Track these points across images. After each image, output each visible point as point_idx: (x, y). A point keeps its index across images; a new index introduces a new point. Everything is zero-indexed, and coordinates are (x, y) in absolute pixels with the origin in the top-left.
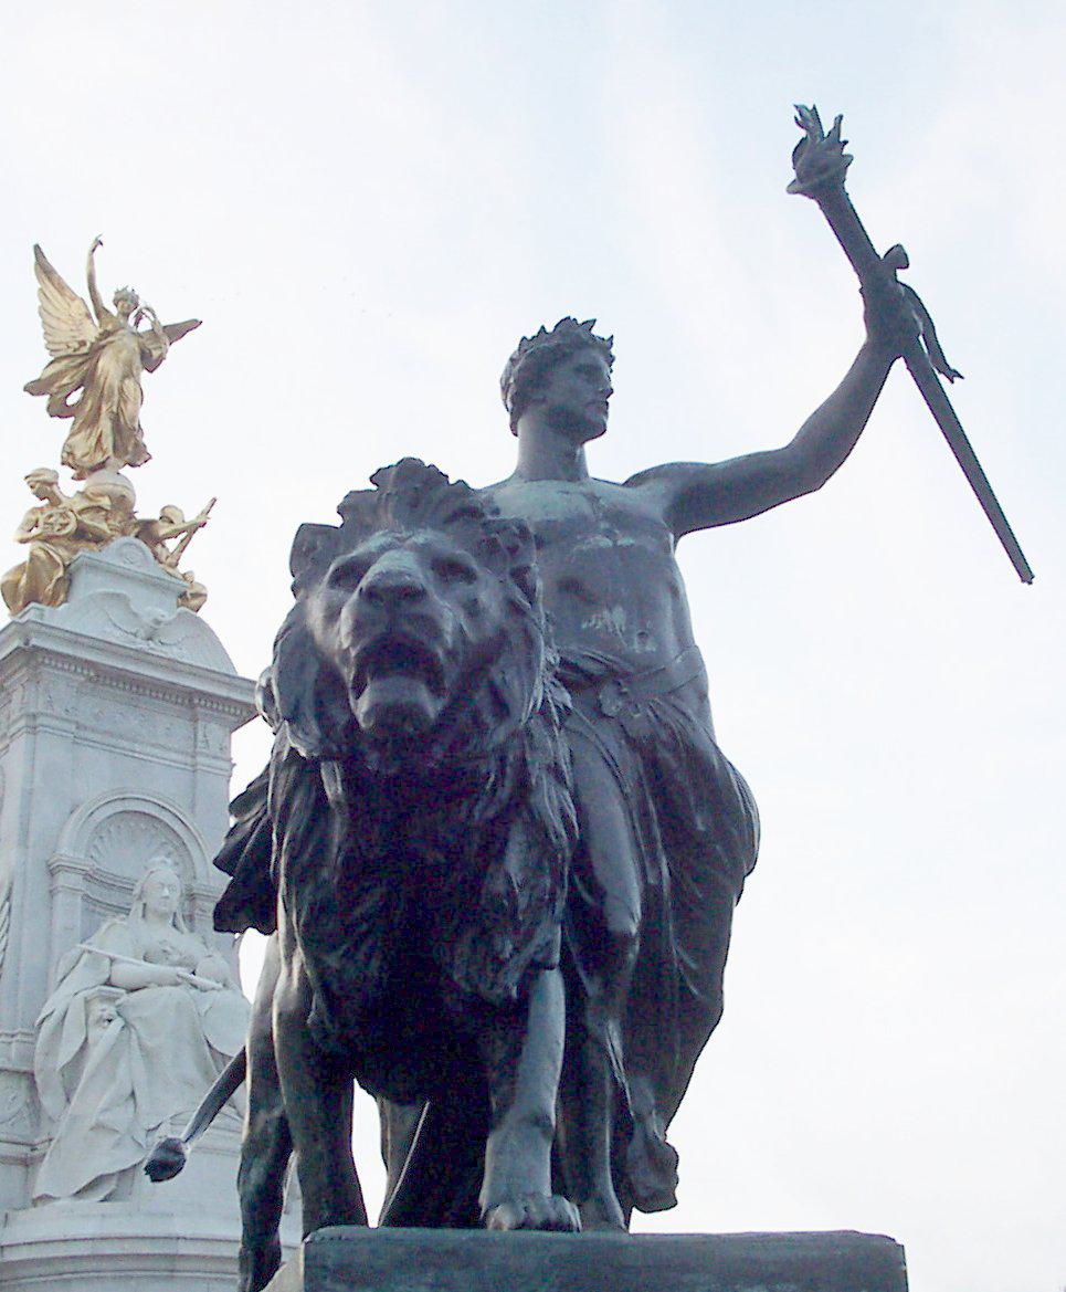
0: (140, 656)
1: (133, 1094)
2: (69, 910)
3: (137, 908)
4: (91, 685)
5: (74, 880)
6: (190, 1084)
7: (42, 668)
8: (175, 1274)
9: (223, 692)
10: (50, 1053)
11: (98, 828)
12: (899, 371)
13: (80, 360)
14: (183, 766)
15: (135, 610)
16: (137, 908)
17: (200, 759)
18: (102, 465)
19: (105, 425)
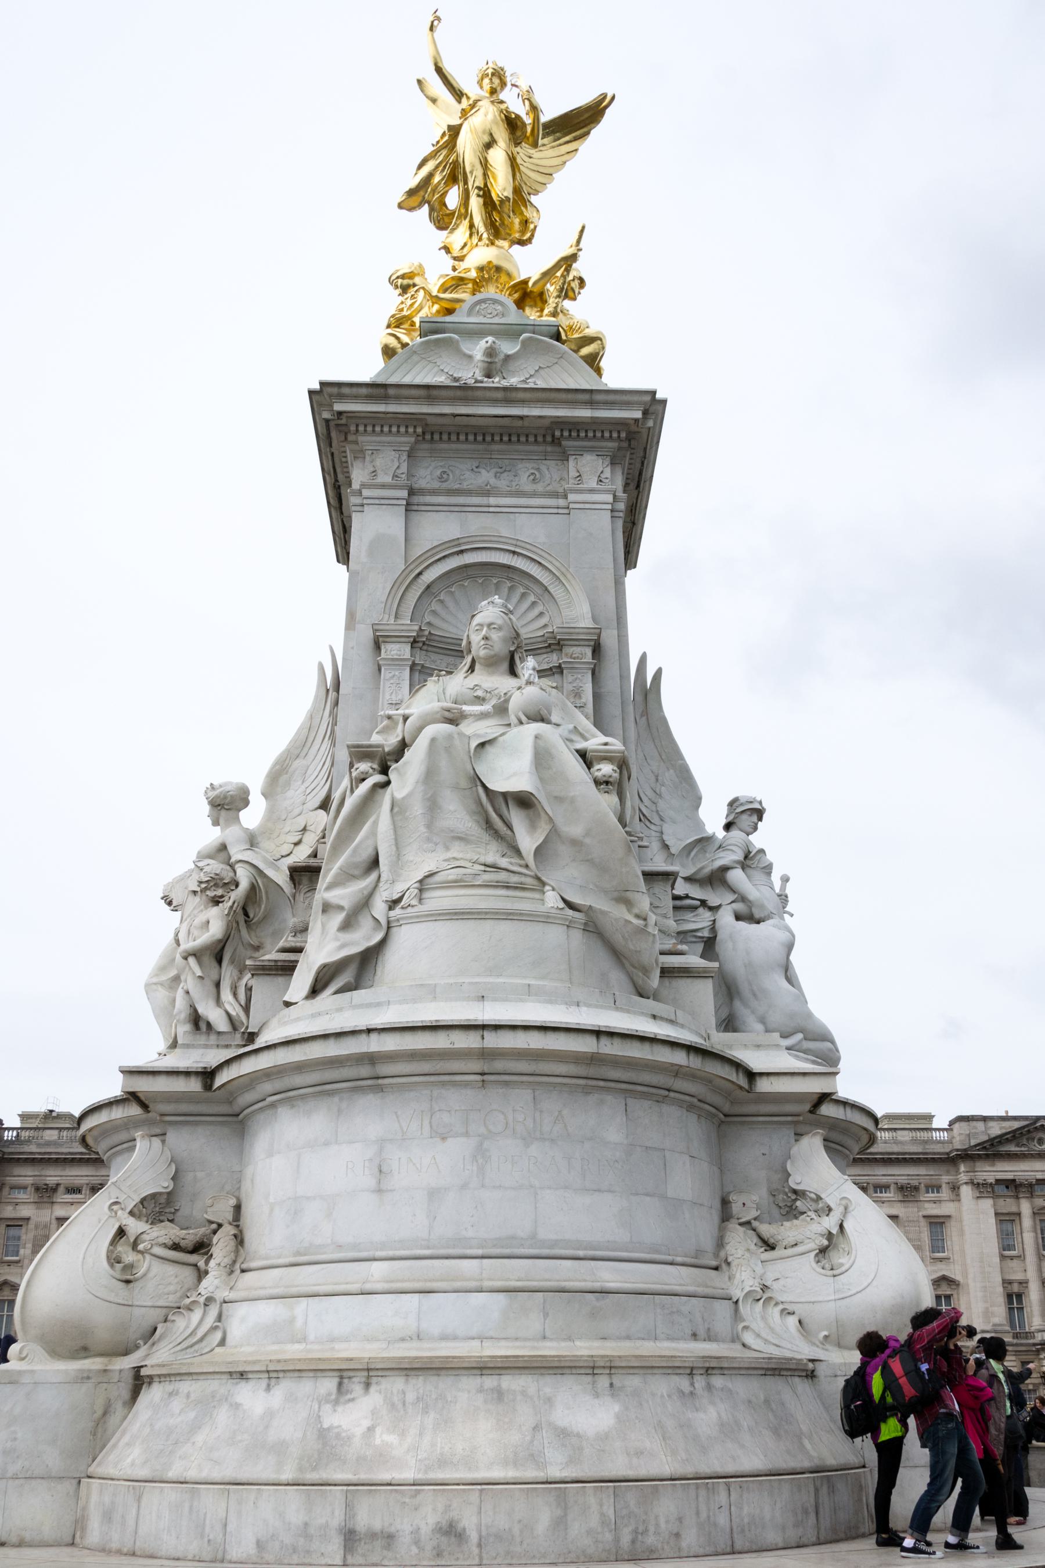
4: (426, 446)
5: (404, 651)
6: (462, 839)
7: (361, 439)
8: (380, 1081)
9: (585, 413)
13: (444, 152)
14: (556, 511)
15: (470, 353)
17: (572, 497)
19: (475, 204)
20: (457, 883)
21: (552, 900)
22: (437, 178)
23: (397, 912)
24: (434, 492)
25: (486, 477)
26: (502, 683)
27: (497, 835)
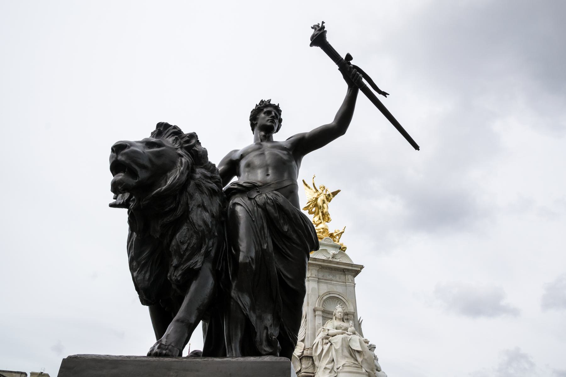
0: (330, 262)
1: (333, 360)
2: (319, 320)
3: (334, 318)
6: (347, 357)
10: (316, 351)
11: (324, 301)
12: (361, 95)
16: (334, 318)
18: (321, 223)
19: (320, 214)
20: (349, 366)
21: (364, 371)
22: (311, 206)
23: (339, 370)
24: (322, 279)
25: (331, 277)
26: (345, 324)
27: (352, 357)
